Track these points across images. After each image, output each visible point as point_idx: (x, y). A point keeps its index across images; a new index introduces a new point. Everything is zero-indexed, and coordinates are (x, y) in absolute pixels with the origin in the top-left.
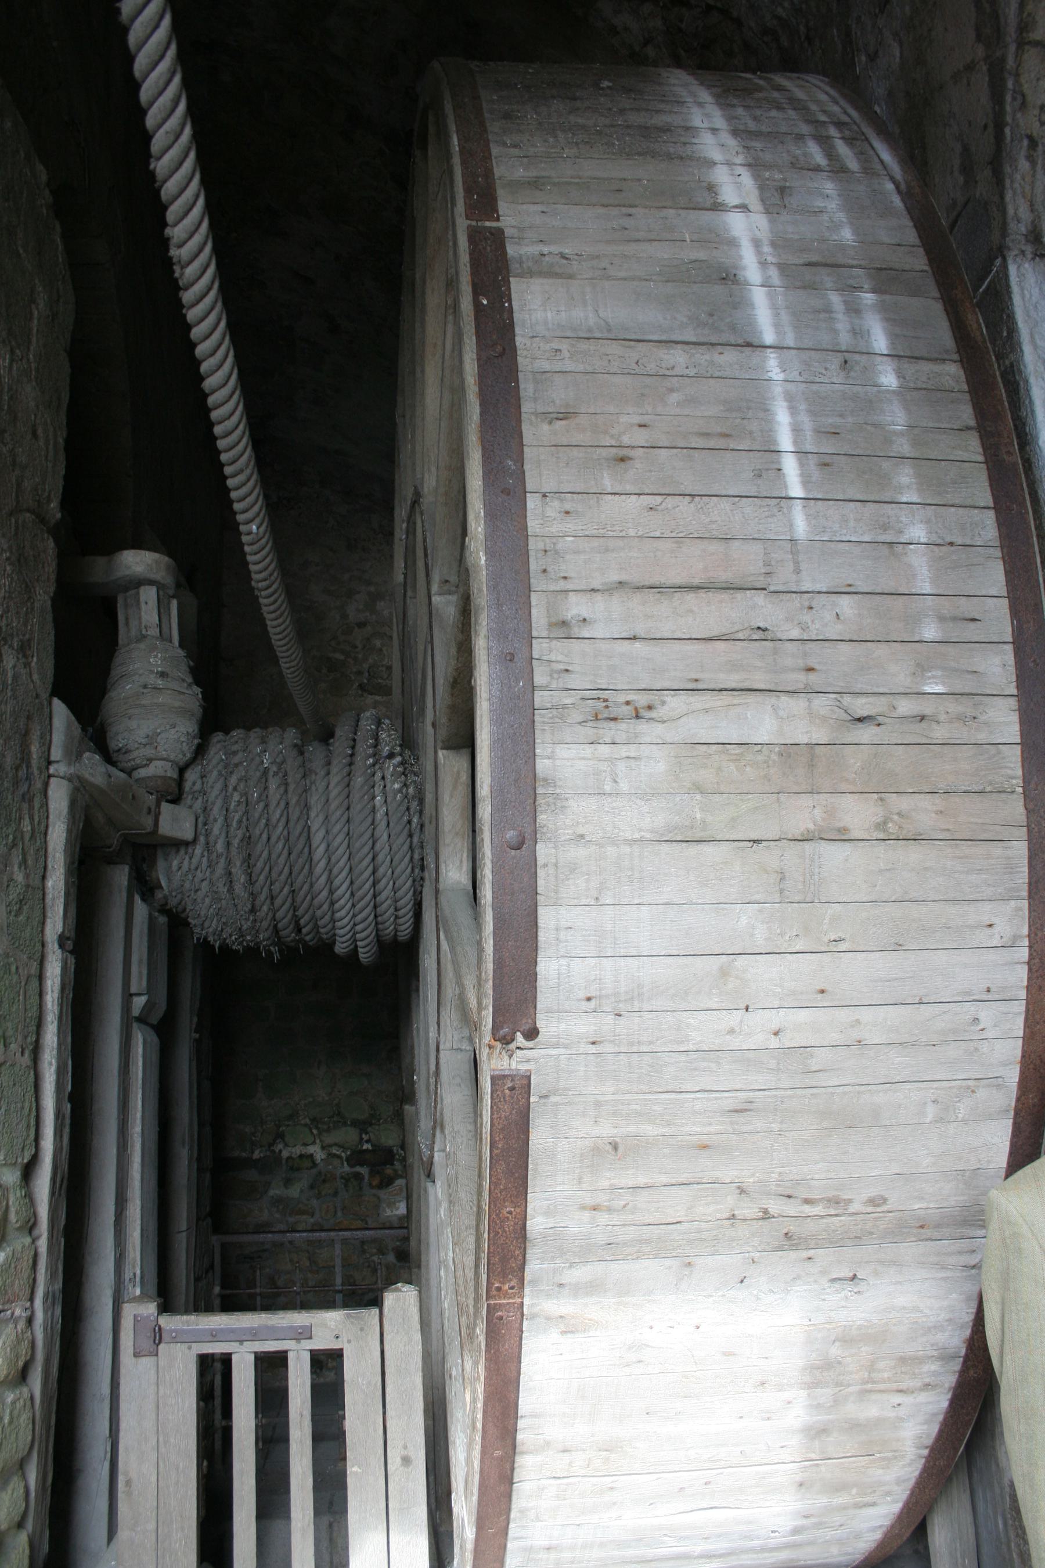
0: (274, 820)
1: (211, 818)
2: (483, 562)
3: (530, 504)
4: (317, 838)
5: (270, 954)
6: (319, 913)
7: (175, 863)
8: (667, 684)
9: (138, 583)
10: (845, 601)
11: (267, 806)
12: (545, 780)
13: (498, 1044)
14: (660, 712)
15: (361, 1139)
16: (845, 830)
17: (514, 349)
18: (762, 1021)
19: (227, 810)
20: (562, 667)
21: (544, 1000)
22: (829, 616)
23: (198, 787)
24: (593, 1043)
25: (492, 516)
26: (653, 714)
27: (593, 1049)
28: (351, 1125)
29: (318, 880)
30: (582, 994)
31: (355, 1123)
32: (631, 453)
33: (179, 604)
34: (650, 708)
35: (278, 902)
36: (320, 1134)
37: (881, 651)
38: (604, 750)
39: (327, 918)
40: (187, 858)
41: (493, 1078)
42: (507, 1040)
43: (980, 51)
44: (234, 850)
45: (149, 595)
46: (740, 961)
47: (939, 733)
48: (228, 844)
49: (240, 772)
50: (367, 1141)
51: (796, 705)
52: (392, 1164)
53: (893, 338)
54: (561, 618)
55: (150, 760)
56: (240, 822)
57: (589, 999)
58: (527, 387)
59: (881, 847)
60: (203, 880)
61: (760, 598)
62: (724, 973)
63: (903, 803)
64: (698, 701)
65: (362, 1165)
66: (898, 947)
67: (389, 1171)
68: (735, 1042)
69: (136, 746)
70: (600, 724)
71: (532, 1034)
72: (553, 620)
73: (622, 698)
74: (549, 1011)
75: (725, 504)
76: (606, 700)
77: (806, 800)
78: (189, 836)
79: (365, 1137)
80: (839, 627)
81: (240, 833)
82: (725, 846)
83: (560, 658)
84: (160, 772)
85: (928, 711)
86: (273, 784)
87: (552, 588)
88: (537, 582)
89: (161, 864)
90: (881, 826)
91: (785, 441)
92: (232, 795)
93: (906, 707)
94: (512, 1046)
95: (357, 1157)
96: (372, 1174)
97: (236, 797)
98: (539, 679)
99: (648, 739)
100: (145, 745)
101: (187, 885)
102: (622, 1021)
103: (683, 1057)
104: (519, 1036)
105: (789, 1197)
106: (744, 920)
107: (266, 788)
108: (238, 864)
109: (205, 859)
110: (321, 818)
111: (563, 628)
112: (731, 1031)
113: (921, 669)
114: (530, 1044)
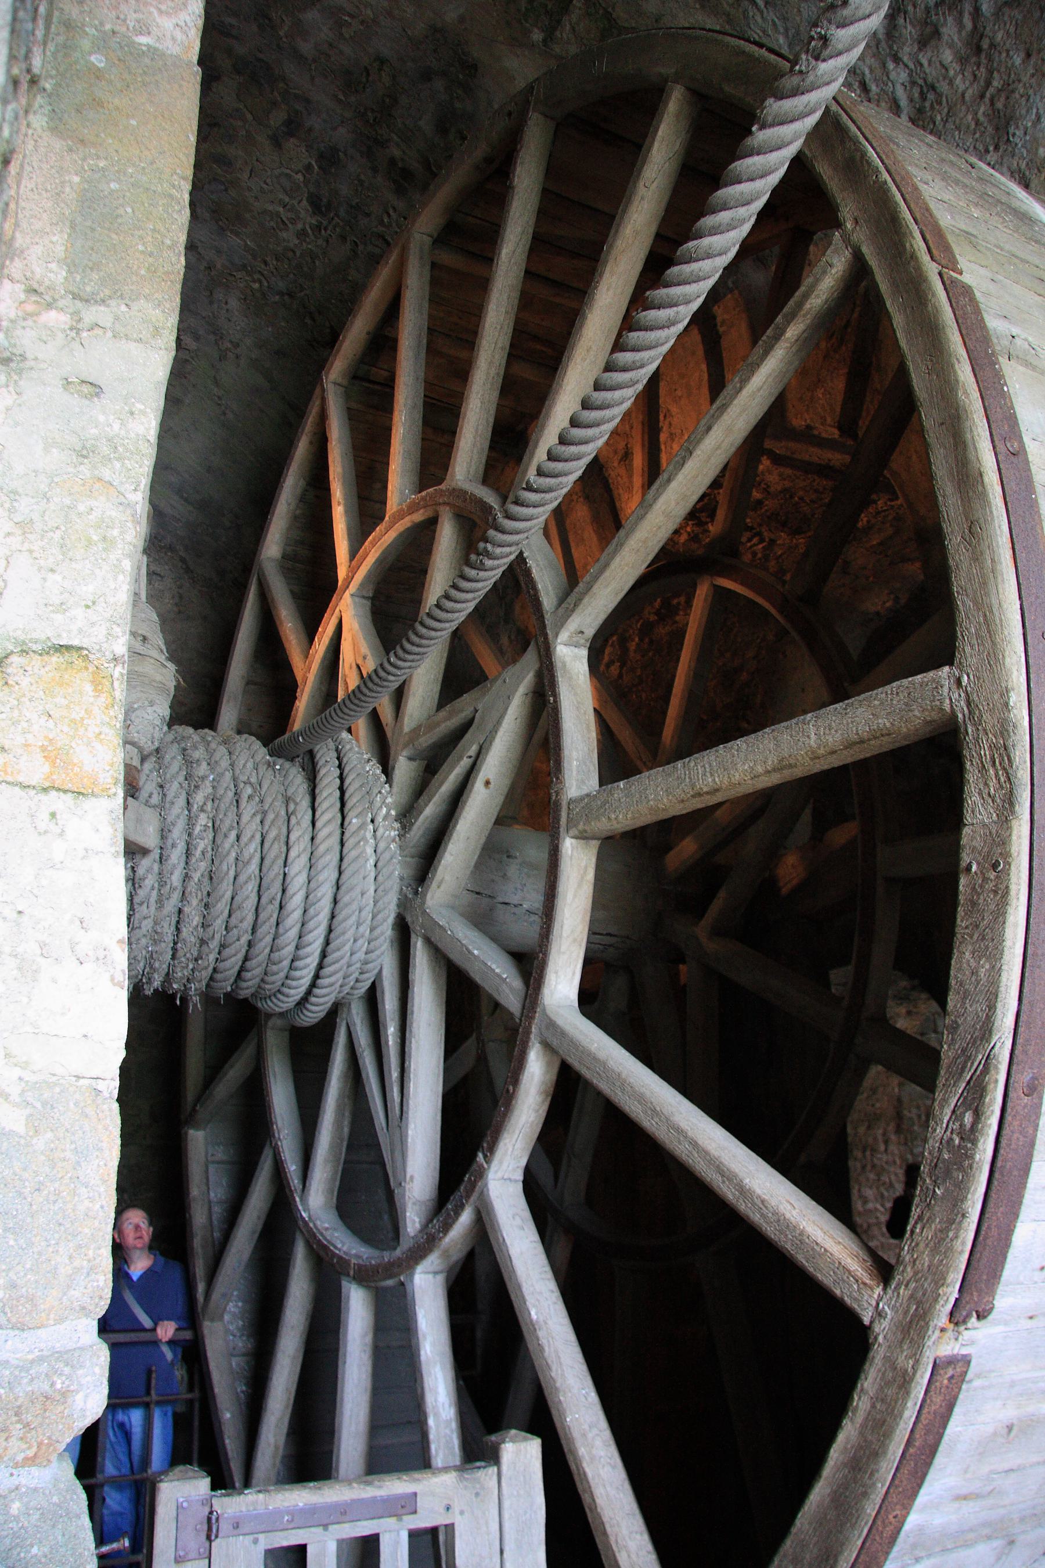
0: (246, 855)
1: (170, 842)
11: (238, 837)
19: (190, 835)
29: (287, 931)
44: (192, 887)
48: (186, 878)
49: (206, 789)
60: (145, 918)
81: (203, 866)
86: (248, 810)
97: (203, 820)
107: (239, 815)
108: (195, 902)
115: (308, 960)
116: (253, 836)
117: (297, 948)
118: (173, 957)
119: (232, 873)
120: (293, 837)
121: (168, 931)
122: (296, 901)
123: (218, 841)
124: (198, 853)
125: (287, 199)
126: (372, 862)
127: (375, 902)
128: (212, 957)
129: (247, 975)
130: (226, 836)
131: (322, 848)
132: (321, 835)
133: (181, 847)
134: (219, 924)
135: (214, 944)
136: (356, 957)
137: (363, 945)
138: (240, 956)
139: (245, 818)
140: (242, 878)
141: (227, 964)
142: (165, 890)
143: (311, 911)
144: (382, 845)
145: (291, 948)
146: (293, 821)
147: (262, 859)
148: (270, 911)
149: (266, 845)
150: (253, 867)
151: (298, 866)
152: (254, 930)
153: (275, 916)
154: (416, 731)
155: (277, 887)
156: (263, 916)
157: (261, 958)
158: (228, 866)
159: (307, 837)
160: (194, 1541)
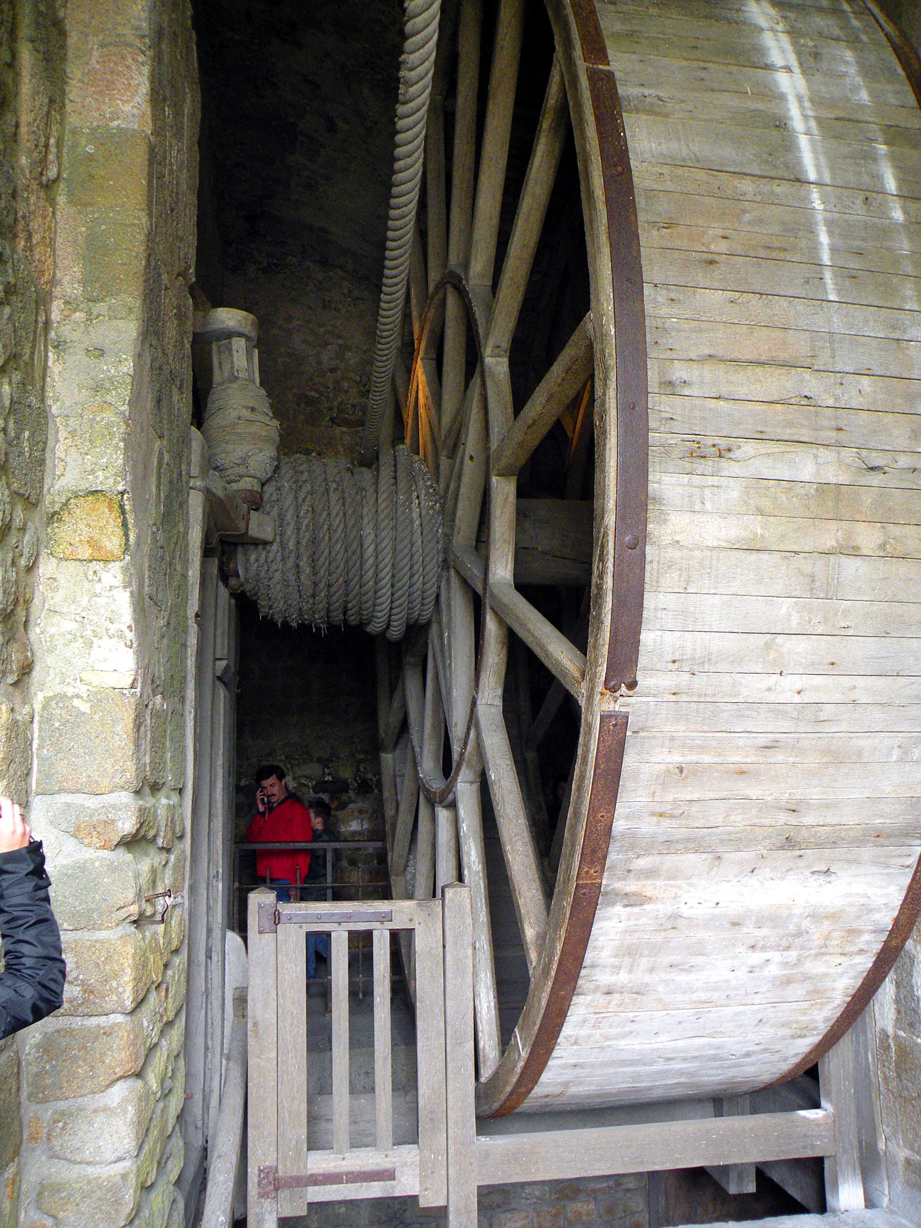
1: (285, 522)
2: (613, 333)
3: (646, 292)
5: (319, 629)
6: (364, 598)
7: (253, 557)
8: (741, 434)
9: (229, 335)
10: (865, 381)
12: (654, 499)
14: (737, 454)
15: (324, 772)
16: (856, 548)
17: (630, 170)
18: (791, 683)
19: (297, 517)
20: (668, 415)
21: (642, 661)
22: (854, 392)
23: (274, 498)
24: (674, 694)
25: (619, 299)
26: (731, 455)
27: (673, 698)
28: (316, 761)
30: (670, 658)
31: (319, 760)
32: (717, 258)
33: (259, 353)
34: (729, 450)
36: (292, 767)
37: (888, 418)
38: (696, 480)
39: (370, 603)
40: (264, 553)
41: (602, 717)
42: (614, 690)
44: (302, 550)
45: (239, 344)
46: (780, 639)
49: (307, 487)
50: (328, 774)
51: (826, 455)
52: (347, 792)
54: (668, 379)
55: (241, 476)
56: (307, 526)
57: (674, 662)
58: (641, 202)
61: (807, 375)
62: (768, 646)
64: (763, 447)
65: (324, 792)
66: (886, 635)
67: (344, 797)
68: (771, 697)
69: (232, 465)
70: (694, 460)
71: (632, 685)
72: (663, 380)
73: (710, 441)
75: (784, 303)
76: (699, 443)
77: (833, 525)
78: (270, 538)
82: (777, 555)
83: (668, 408)
84: (249, 487)
86: (334, 497)
87: (662, 356)
88: (652, 352)
89: (240, 557)
90: (882, 547)
93: (904, 461)
94: (618, 694)
95: (321, 786)
96: (332, 798)
98: (652, 424)
99: (726, 473)
100: (239, 465)
101: (263, 574)
102: (695, 678)
103: (735, 707)
105: (794, 811)
106: (784, 610)
108: (305, 559)
111: (669, 386)
112: (769, 689)
114: (631, 693)
116: (338, 513)
119: (327, 538)
121: (292, 577)
130: (320, 515)
139: (333, 503)
140: (333, 540)
153: (358, 563)
157: (355, 592)
160: (268, 925)
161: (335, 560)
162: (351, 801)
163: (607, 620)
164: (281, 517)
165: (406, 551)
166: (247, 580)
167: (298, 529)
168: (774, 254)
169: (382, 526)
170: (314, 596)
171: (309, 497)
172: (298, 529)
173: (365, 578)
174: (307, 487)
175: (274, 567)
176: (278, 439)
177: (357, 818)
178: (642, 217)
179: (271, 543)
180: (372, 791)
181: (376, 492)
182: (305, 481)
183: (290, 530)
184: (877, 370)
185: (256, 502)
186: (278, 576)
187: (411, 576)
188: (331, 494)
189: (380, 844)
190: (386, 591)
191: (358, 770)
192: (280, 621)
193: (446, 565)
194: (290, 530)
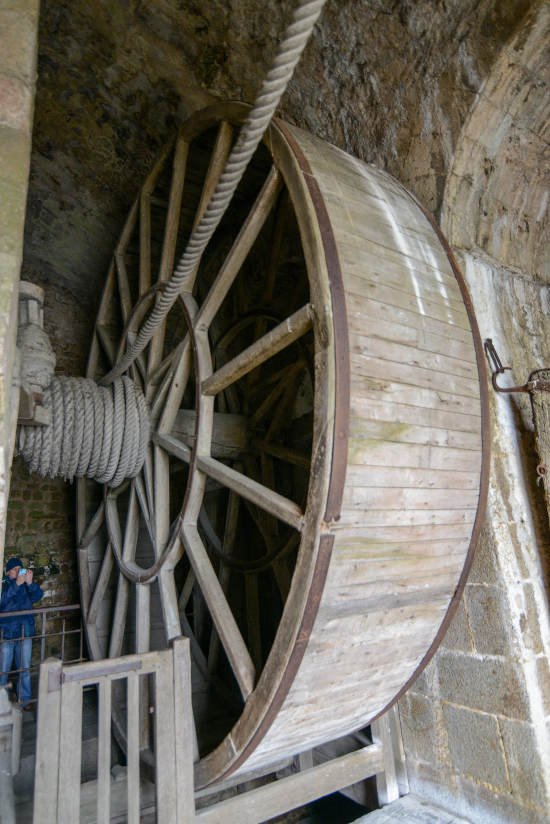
0: (88, 419)
1: (56, 415)
4: (109, 429)
7: (32, 435)
10: (438, 358)
11: (84, 413)
13: (325, 523)
15: (29, 563)
16: (437, 442)
18: (409, 514)
20: (357, 365)
30: (356, 502)
35: (83, 457)
37: (447, 376)
38: (370, 402)
43: (433, 172)
45: (33, 305)
47: (463, 410)
48: (64, 428)
49: (71, 395)
53: (438, 264)
56: (71, 418)
58: (339, 248)
59: (447, 450)
61: (416, 351)
63: (452, 434)
66: (447, 488)
67: (41, 577)
68: (400, 523)
71: (338, 518)
73: (377, 381)
74: (345, 509)
77: (427, 430)
79: (31, 562)
80: (436, 365)
81: (71, 423)
82: (406, 445)
85: (460, 401)
86: (88, 402)
90: (447, 442)
91: (418, 293)
92: (67, 405)
93: (455, 398)
94: (329, 524)
97: (70, 406)
98: (352, 369)
100: (31, 376)
101: (38, 445)
104: (333, 519)
106: (407, 475)
107: (84, 404)
109: (51, 436)
110: (111, 420)
112: (399, 519)
113: (458, 385)
115: (115, 458)
117: (111, 454)
118: (61, 460)
119: (83, 426)
120: (106, 412)
121: (57, 449)
122: (108, 436)
123: (77, 414)
124: (68, 419)
125: (106, 150)
126: (138, 420)
127: (140, 436)
128: (77, 459)
129: (92, 466)
131: (118, 415)
132: (117, 411)
133: (61, 417)
134: (78, 446)
135: (77, 454)
136: (134, 457)
137: (136, 452)
138: (89, 458)
139: (87, 406)
140: (87, 428)
141: (83, 462)
142: (56, 433)
143: (115, 439)
144: (141, 415)
145: (108, 454)
146: (106, 406)
147: (95, 420)
148: (99, 440)
149: (96, 415)
150: (91, 423)
151: (109, 423)
152: (93, 448)
154: (154, 372)
155: (100, 431)
156: (96, 442)
158: (80, 423)
159: (112, 412)
161: (87, 439)
162: (45, 579)
163: (327, 480)
164: (54, 412)
165: (131, 436)
166: (26, 450)
167: (64, 420)
168: (397, 287)
169: (117, 421)
170: (71, 460)
171: (72, 401)
172: (64, 420)
173: (104, 451)
174: (71, 395)
175: (47, 442)
176: (55, 364)
177: (48, 589)
178: (341, 257)
179: (47, 426)
180: (59, 572)
181: (114, 401)
182: (69, 392)
183: (59, 420)
184: (442, 352)
185: (39, 402)
186: (49, 447)
187: (132, 451)
188: (86, 400)
189: (77, 607)
190: (116, 458)
191: (51, 560)
192: (45, 475)
193: (152, 446)
194: (59, 420)
